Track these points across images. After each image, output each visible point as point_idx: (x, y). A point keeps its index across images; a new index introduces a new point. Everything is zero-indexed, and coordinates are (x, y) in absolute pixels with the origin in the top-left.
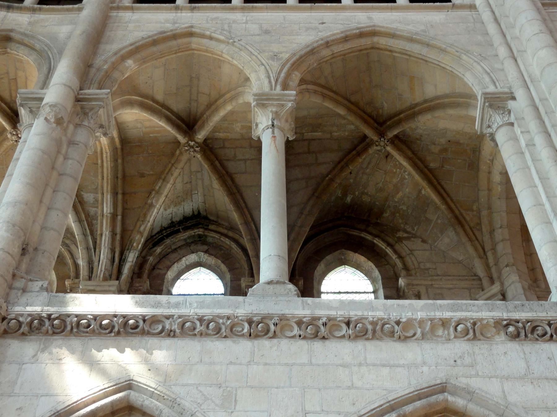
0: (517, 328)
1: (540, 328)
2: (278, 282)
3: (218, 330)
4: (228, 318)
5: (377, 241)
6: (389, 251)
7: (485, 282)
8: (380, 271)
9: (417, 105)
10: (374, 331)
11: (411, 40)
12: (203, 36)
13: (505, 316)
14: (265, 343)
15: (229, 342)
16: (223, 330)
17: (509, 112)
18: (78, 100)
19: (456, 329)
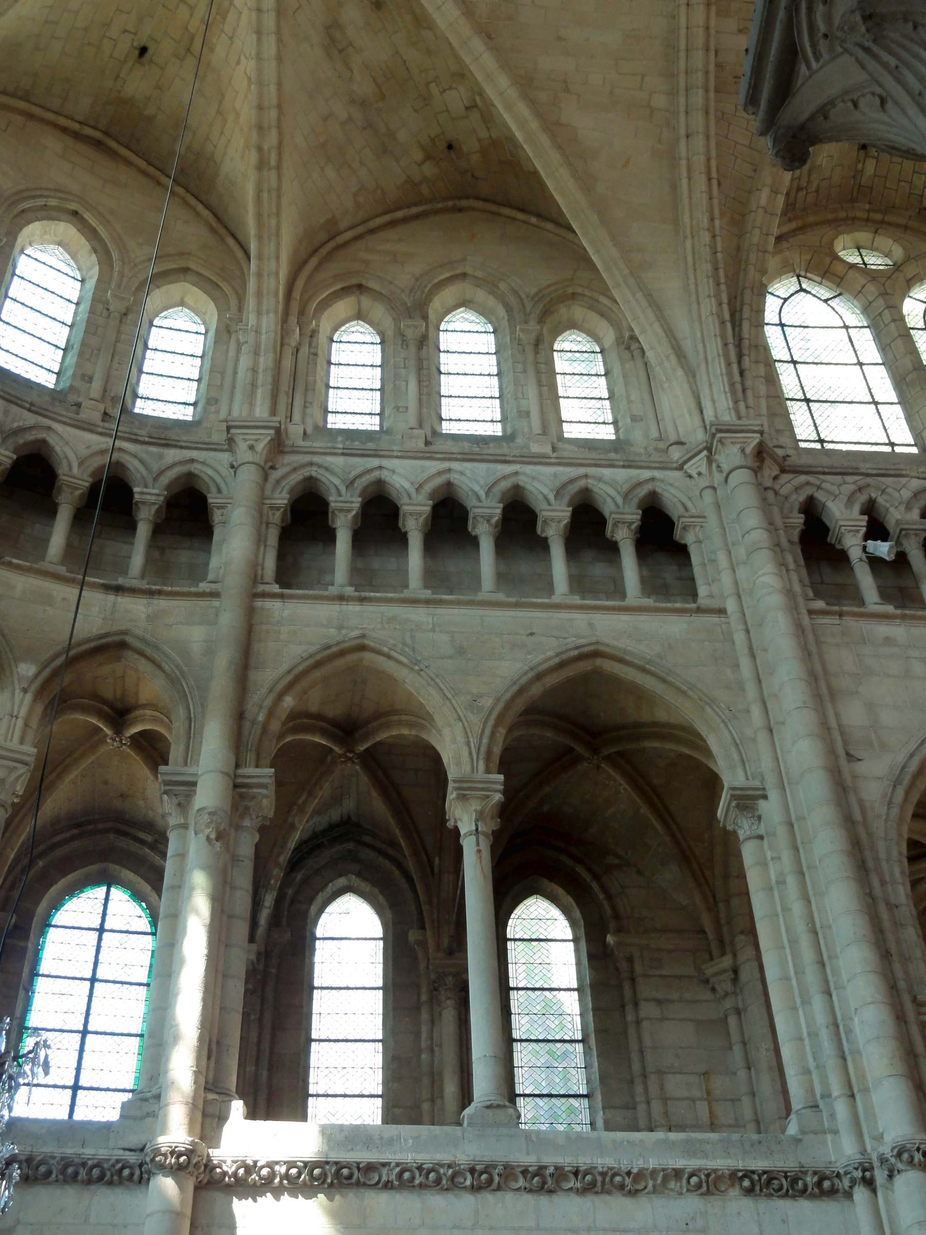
0: (752, 1182)
1: (776, 1182)
2: (498, 1106)
3: (438, 1181)
4: (449, 1166)
5: (579, 869)
6: (595, 886)
7: (716, 952)
8: (581, 913)
9: (642, 725)
10: (603, 1182)
11: (643, 670)
12: (378, 652)
13: (741, 1165)
14: (488, 1198)
15: (450, 1196)
16: (444, 1182)
17: (759, 818)
18: (236, 786)
19: (688, 1182)
